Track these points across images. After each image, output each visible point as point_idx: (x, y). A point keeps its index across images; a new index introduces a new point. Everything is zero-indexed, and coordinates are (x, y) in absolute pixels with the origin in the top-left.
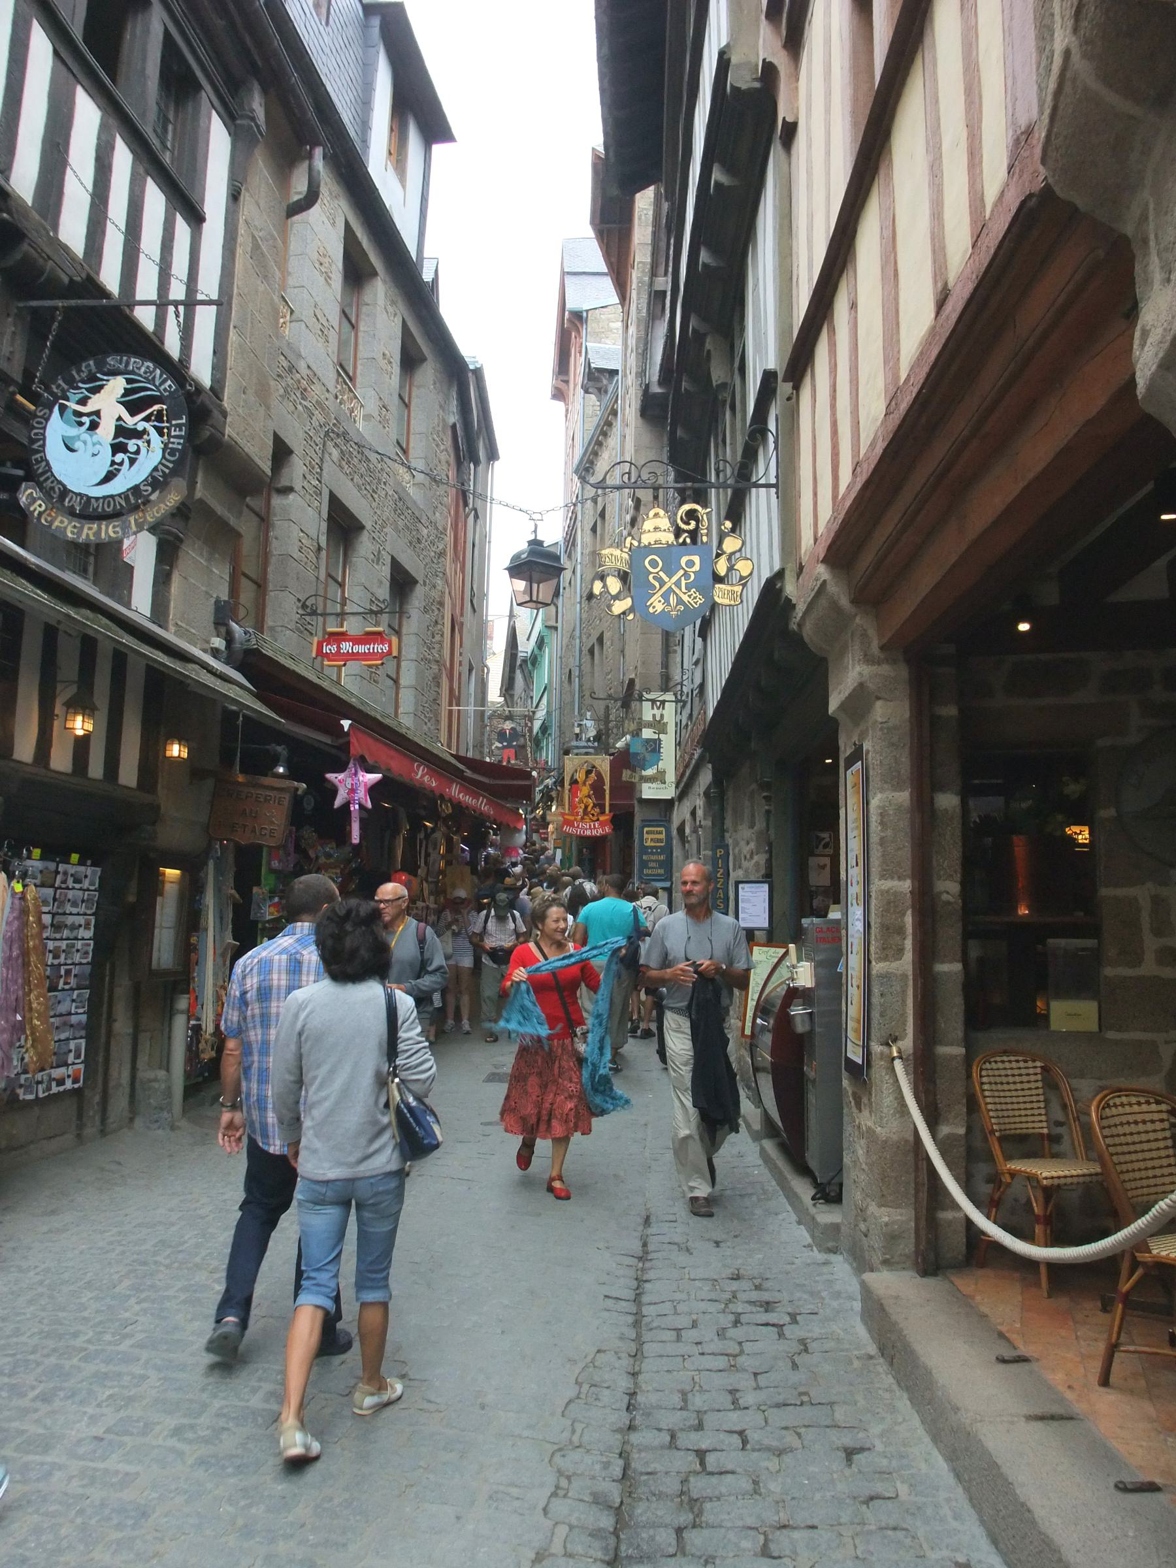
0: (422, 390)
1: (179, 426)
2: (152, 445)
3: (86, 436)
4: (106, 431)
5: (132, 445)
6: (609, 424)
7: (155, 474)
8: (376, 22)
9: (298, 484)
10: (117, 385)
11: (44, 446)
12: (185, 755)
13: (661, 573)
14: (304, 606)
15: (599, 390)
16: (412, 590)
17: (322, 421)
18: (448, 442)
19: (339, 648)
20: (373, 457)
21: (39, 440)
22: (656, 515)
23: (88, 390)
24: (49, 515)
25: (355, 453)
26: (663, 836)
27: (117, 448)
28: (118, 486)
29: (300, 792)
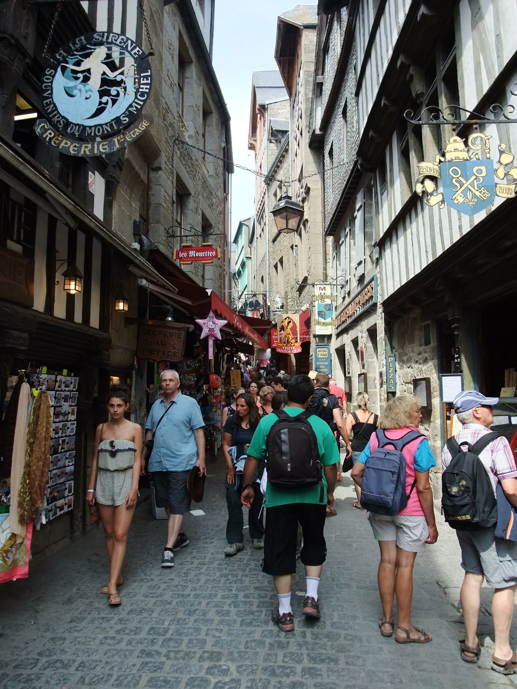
0: (211, 128)
1: (146, 77)
2: (127, 90)
3: (81, 86)
4: (95, 82)
5: (113, 91)
6: (283, 156)
7: (130, 109)
9: (163, 166)
10: (101, 52)
11: (51, 94)
12: (126, 309)
13: (460, 178)
15: (276, 141)
17: (173, 134)
19: (188, 254)
21: (48, 90)
22: (455, 141)
24: (57, 139)
26: (327, 353)
27: (102, 93)
28: (105, 118)
29: (190, 330)
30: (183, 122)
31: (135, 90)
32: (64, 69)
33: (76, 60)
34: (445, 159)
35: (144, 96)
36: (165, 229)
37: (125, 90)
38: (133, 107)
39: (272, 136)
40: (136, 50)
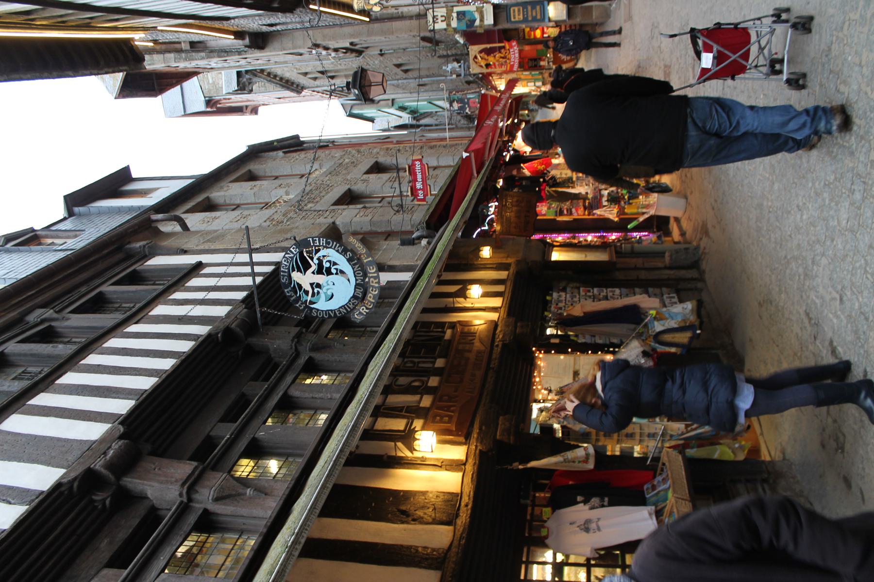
0: (267, 170)
1: (314, 241)
2: (326, 254)
3: (324, 289)
4: (320, 279)
5: (326, 265)
6: (269, 74)
7: (340, 251)
8: (76, 210)
10: (296, 276)
11: (331, 311)
14: (398, 211)
15: (250, 83)
16: (381, 164)
18: (294, 154)
20: (308, 189)
23: (300, 291)
25: (308, 196)
27: (329, 272)
30: (274, 203)
32: (312, 303)
35: (329, 242)
36: (395, 214)
37: (326, 256)
39: (245, 90)
40: (293, 250)
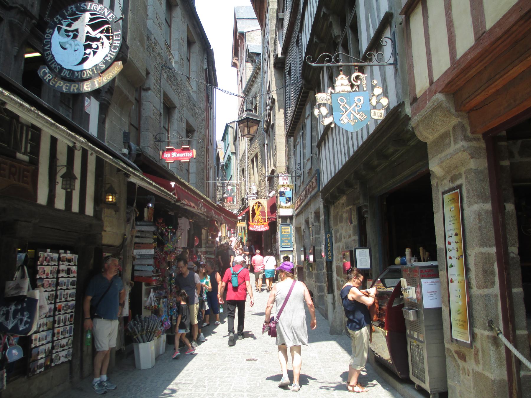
1: (118, 35)
3: (71, 42)
4: (82, 39)
5: (94, 45)
6: (257, 73)
7: (106, 58)
9: (152, 87)
11: (50, 47)
13: (346, 105)
14: (156, 138)
15: (252, 61)
17: (160, 61)
18: (204, 76)
19: (171, 155)
21: (48, 44)
22: (342, 78)
23: (71, 19)
24: (54, 81)
30: (170, 51)
31: (110, 45)
32: (59, 29)
33: (68, 22)
34: (335, 91)
36: (154, 136)
37: (103, 45)
38: (108, 57)
40: (110, 16)
